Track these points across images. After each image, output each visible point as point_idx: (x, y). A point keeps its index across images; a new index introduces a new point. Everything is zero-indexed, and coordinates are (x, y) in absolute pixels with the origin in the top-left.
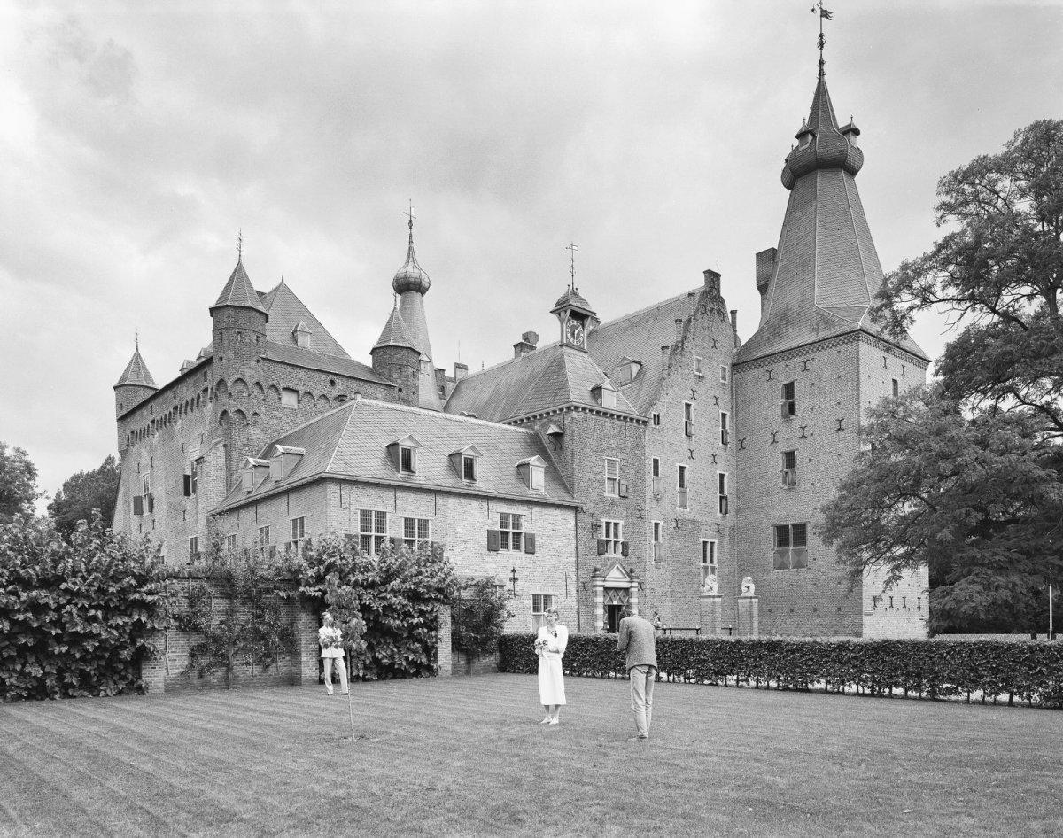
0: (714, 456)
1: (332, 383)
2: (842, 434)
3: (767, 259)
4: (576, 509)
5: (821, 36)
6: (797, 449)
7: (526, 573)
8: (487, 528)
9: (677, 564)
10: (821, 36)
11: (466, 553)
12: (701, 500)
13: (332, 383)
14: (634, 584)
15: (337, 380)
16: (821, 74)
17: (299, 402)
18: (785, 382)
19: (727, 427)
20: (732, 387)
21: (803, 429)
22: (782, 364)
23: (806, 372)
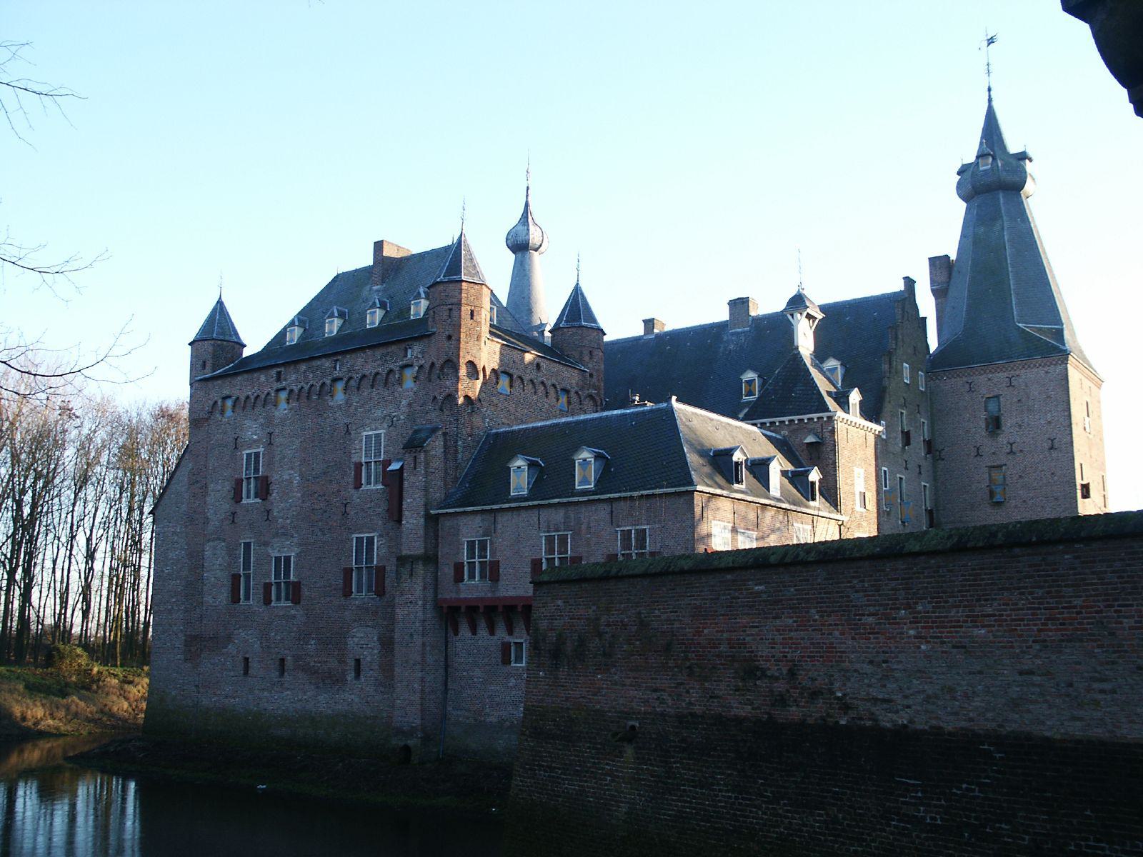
2: (1055, 454)
6: (1005, 465)
16: (990, 100)
18: (988, 396)
22: (983, 378)
23: (1011, 388)
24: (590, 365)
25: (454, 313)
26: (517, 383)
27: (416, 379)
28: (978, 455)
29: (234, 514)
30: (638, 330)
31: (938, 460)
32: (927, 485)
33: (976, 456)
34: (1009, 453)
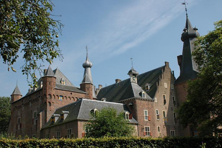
0: (172, 108)
1: (71, 94)
3: (179, 58)
4: (137, 124)
5: (186, 9)
10: (186, 9)
13: (71, 94)
15: (72, 93)
16: (187, 17)
17: (63, 99)
19: (175, 100)
24: (88, 92)
25: (46, 84)
26: (65, 98)
27: (41, 99)
29: (17, 132)
30: (114, 82)
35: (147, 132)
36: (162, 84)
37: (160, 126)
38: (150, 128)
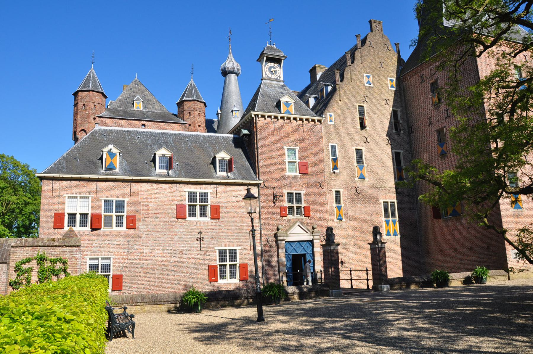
6: (445, 127)
7: (211, 234)
8: (176, 203)
9: (358, 220)
11: (157, 222)
12: (378, 171)
14: (315, 237)
19: (399, 118)
20: (400, 93)
21: (447, 111)
24: (189, 120)
28: (430, 124)
31: (411, 133)
32: (402, 152)
33: (429, 125)
34: (446, 118)
35: (295, 205)
36: (353, 77)
37: (342, 191)
38: (306, 194)
